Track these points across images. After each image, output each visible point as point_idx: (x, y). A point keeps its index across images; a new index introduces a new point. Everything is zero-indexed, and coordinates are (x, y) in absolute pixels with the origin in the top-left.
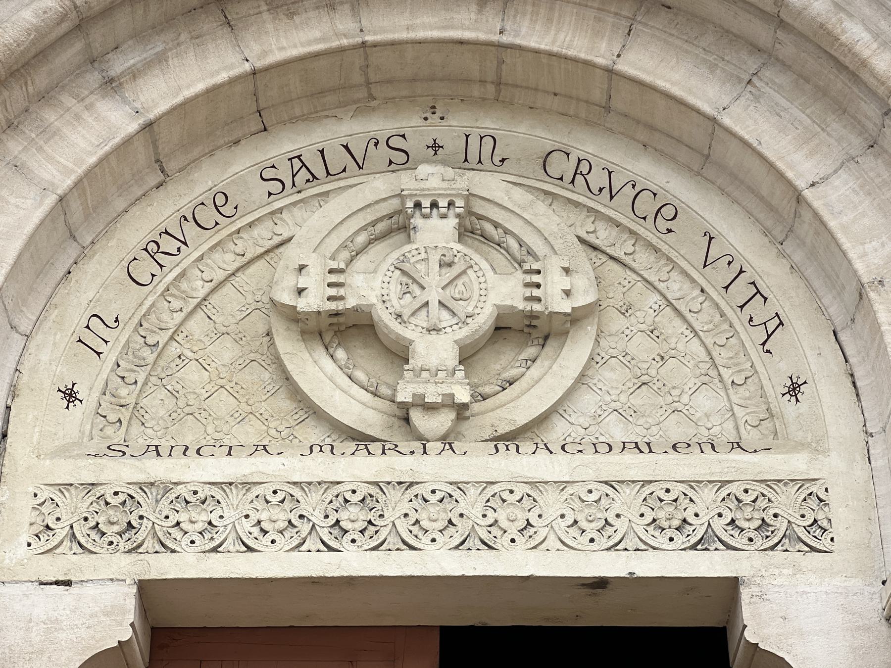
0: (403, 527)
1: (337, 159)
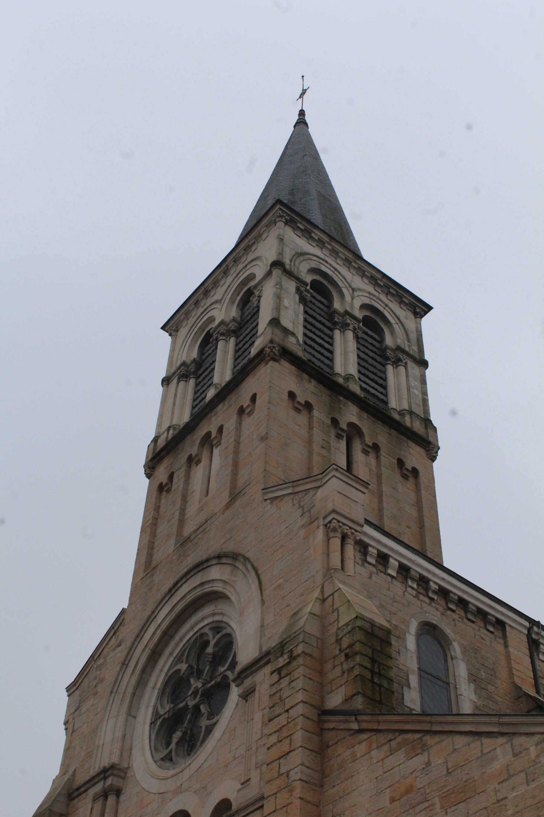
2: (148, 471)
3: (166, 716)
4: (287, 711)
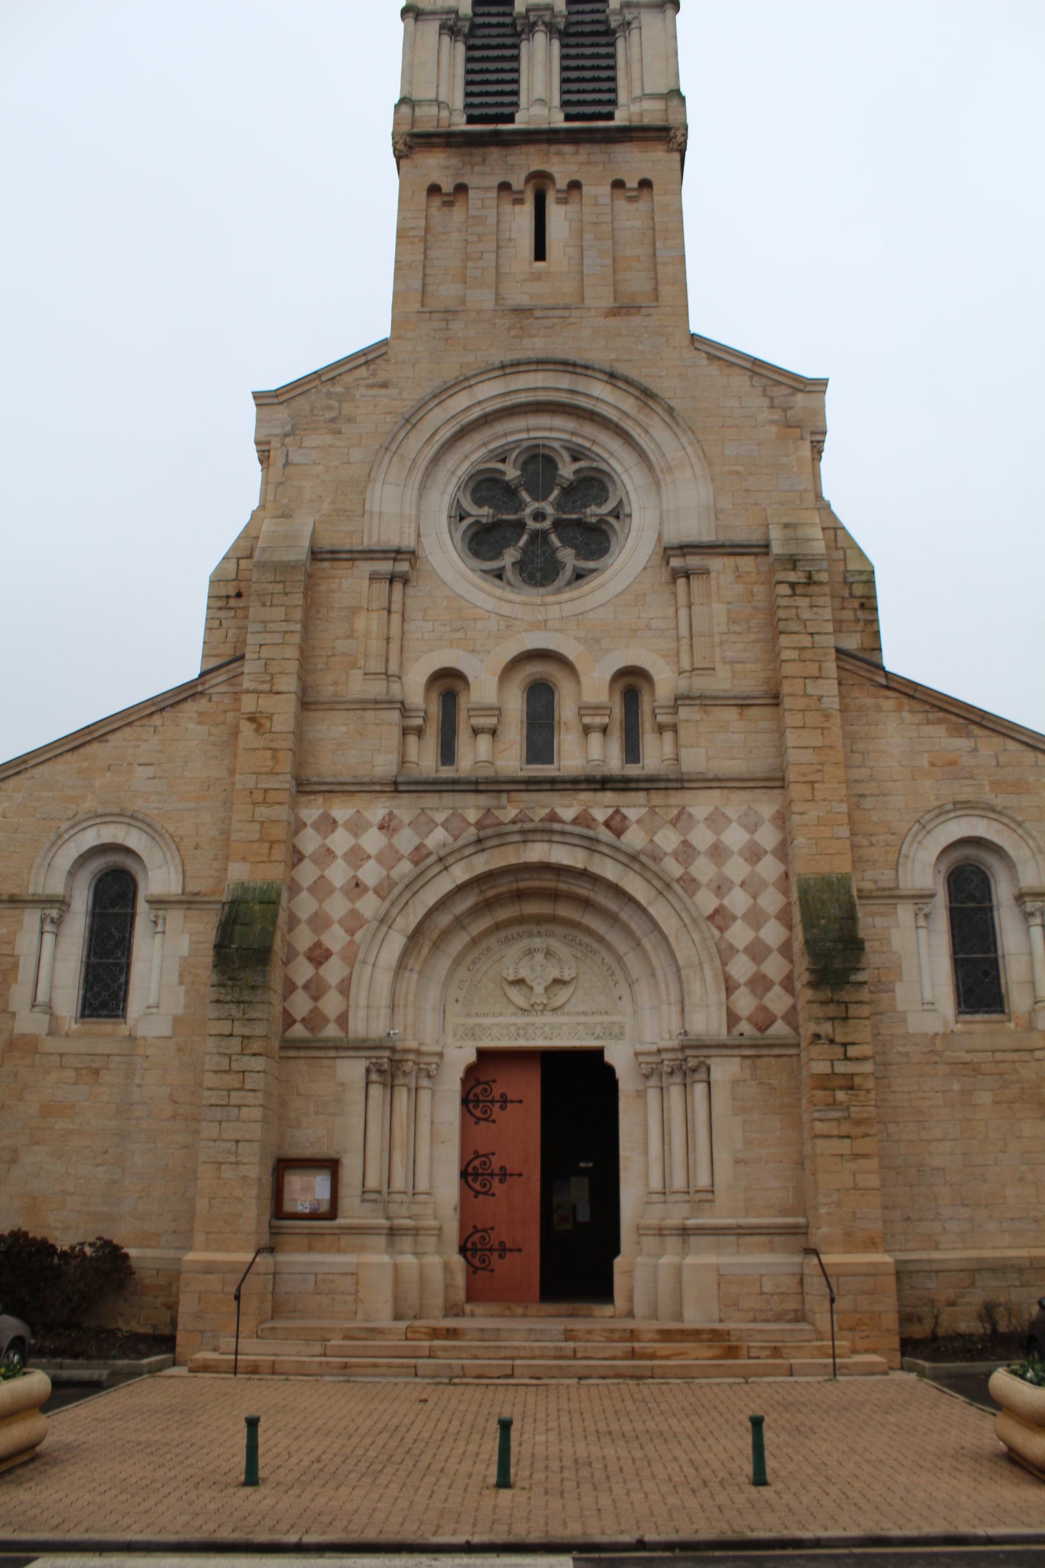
1: (515, 935)
2: (400, 147)
3: (484, 520)
4: (812, 634)
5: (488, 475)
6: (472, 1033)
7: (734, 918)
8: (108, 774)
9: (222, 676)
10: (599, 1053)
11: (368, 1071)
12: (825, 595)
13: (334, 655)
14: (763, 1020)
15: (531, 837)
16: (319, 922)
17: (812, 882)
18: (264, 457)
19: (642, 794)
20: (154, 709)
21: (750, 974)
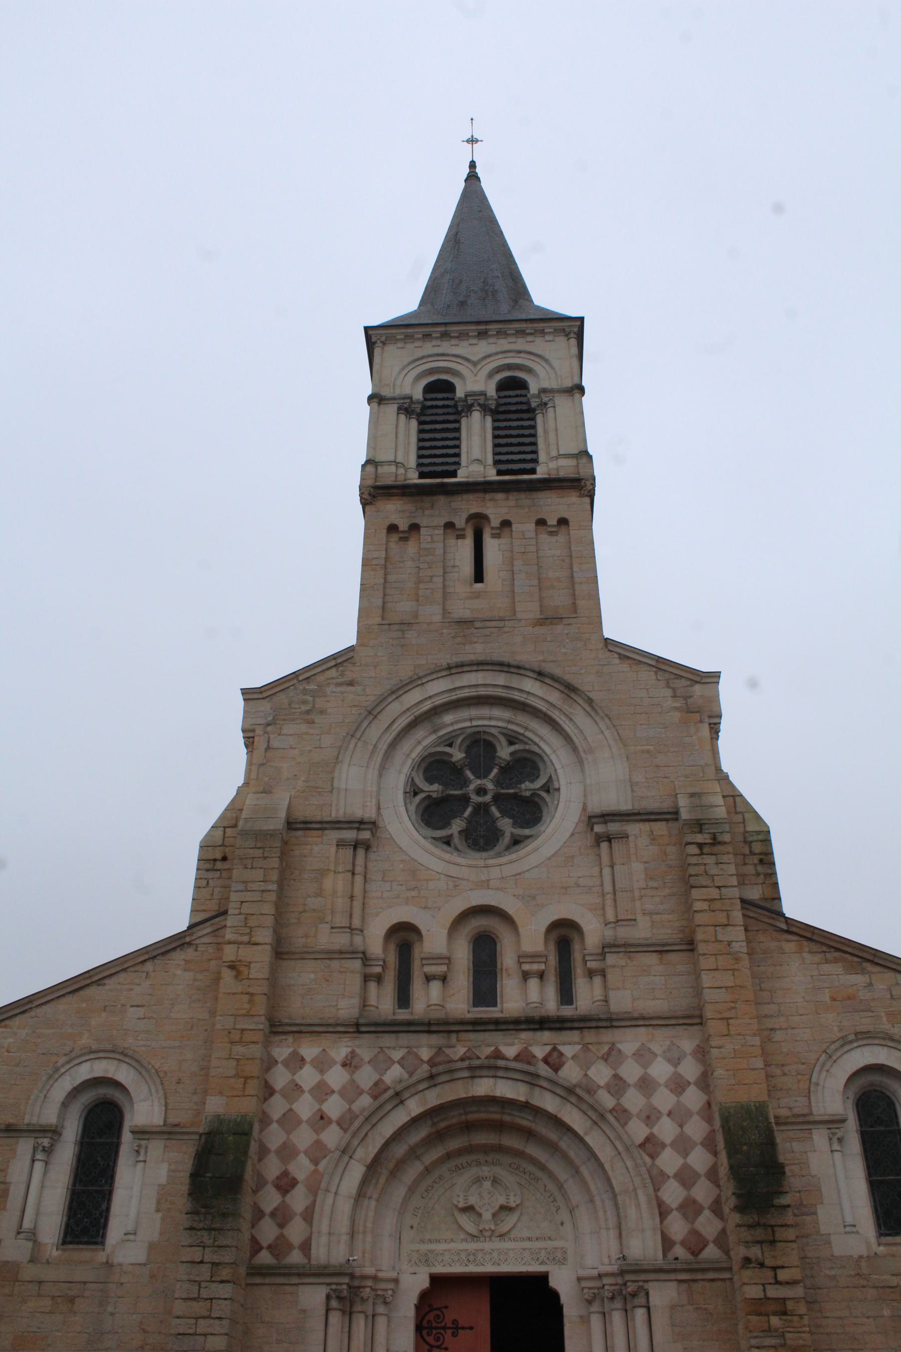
0: (481, 1260)
2: (366, 496)
3: (434, 795)
4: (719, 887)
5: (438, 758)
6: (426, 1259)
7: (663, 1146)
8: (104, 1014)
9: (207, 929)
10: (543, 1278)
11: (328, 1297)
12: (728, 853)
13: (305, 911)
14: (696, 1243)
15: (478, 1073)
16: (287, 1152)
17: (732, 1111)
18: (249, 742)
19: (576, 1032)
20: (147, 957)
21: (680, 1200)
